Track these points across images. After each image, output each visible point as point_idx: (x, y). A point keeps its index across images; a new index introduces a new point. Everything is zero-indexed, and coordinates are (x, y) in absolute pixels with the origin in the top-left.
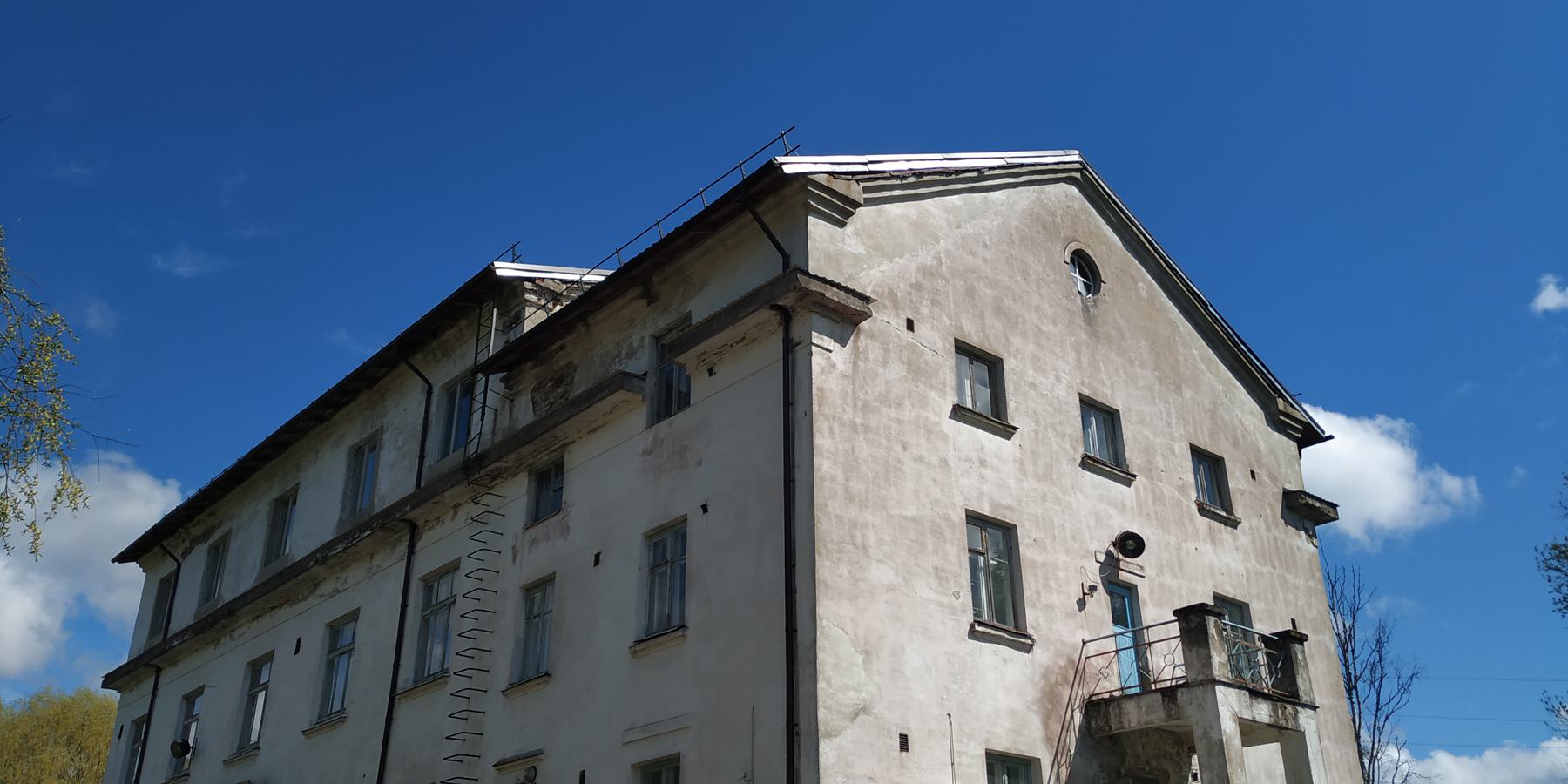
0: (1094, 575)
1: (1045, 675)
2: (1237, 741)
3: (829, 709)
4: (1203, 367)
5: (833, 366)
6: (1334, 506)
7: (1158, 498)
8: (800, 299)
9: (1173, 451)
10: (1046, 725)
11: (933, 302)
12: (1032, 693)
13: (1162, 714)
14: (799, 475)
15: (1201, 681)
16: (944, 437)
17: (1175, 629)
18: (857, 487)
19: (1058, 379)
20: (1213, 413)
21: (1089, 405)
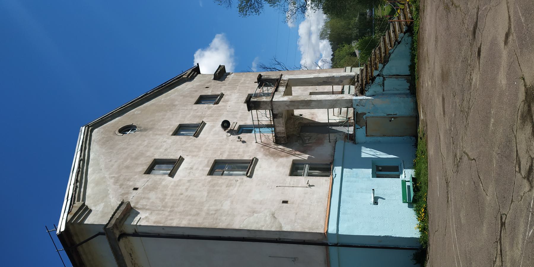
0: (235, 137)
1: (266, 155)
2: (291, 97)
3: (272, 227)
4: (168, 97)
5: (146, 217)
6: (220, 66)
7: (211, 116)
8: (117, 228)
9: (196, 110)
10: (282, 157)
11: (128, 180)
12: (272, 160)
13: (281, 119)
14: (187, 233)
15: (271, 106)
16: (180, 180)
17: (254, 112)
18: (194, 211)
19: (165, 142)
20: (185, 96)
21: (176, 133)
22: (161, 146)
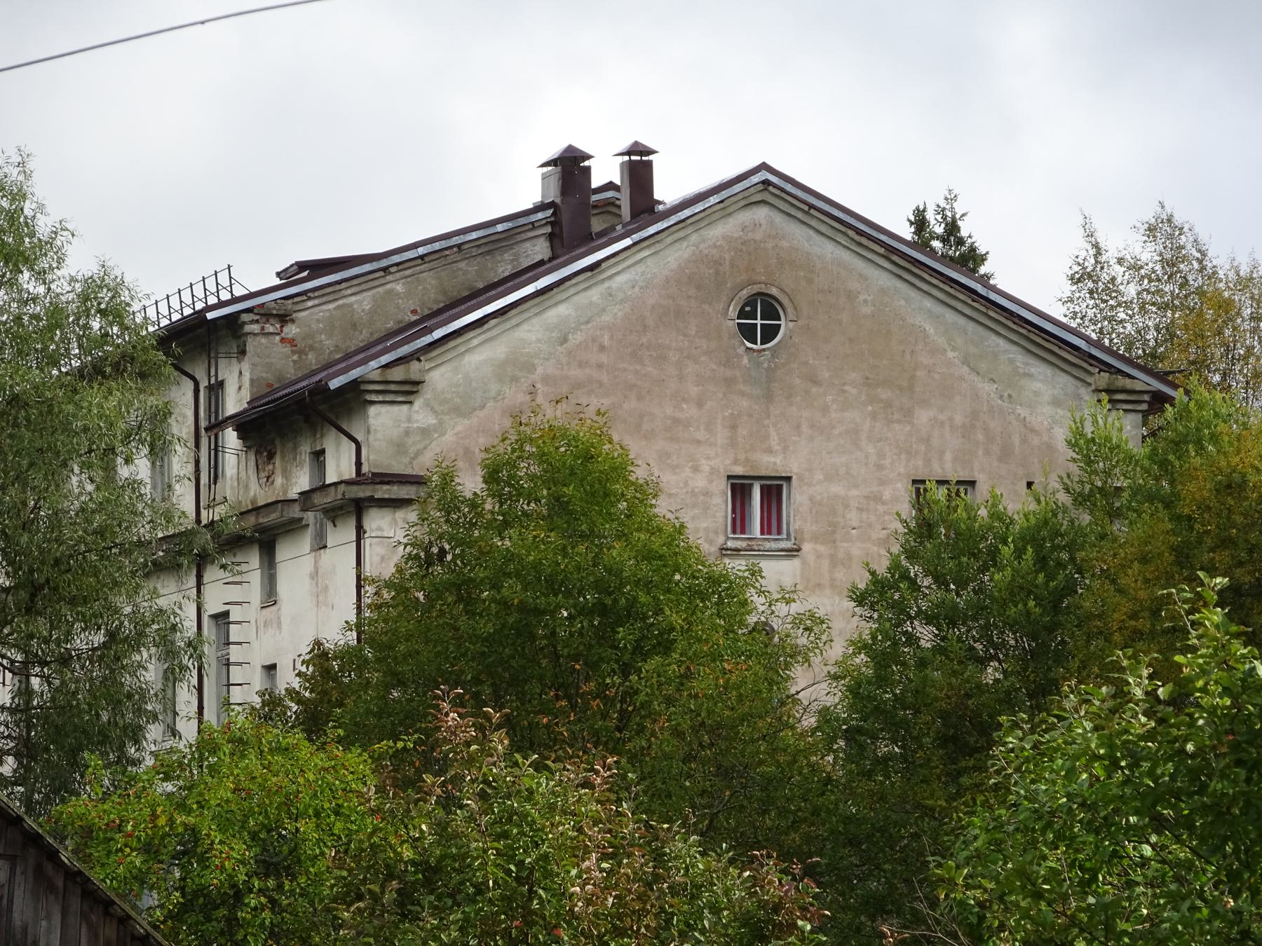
9: (878, 499)
19: (696, 469)
22: (674, 469)
